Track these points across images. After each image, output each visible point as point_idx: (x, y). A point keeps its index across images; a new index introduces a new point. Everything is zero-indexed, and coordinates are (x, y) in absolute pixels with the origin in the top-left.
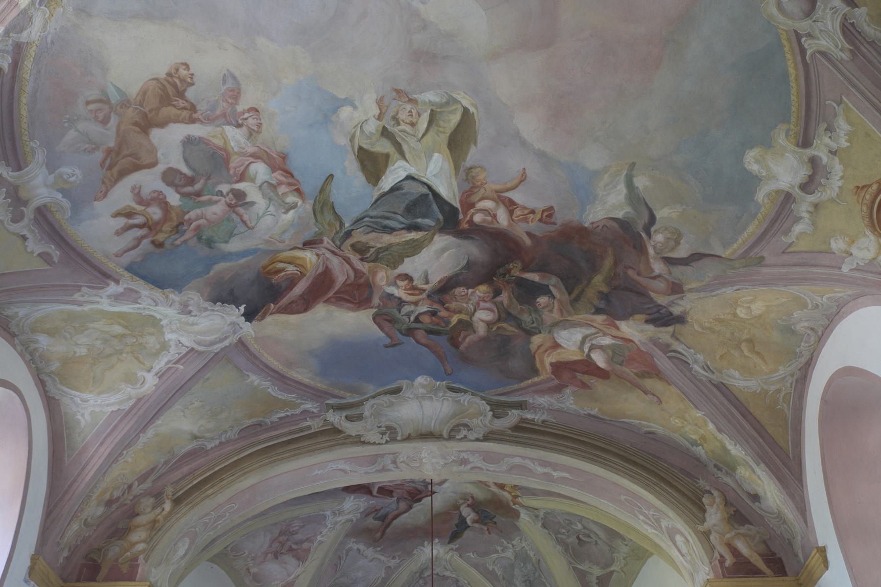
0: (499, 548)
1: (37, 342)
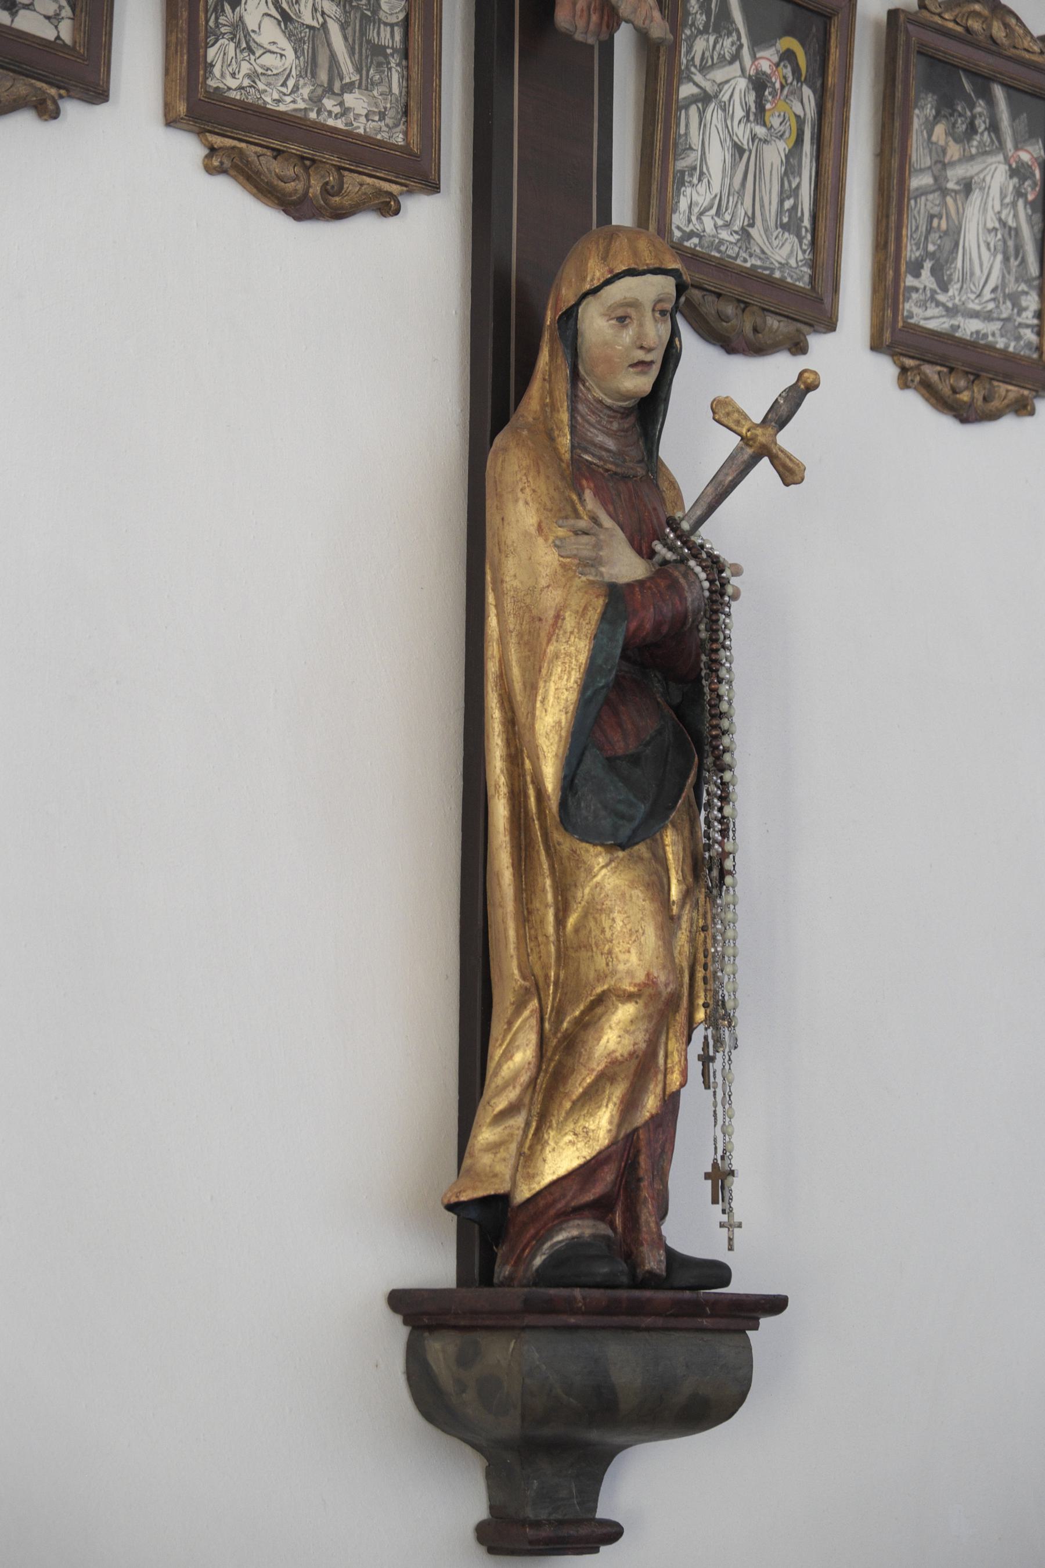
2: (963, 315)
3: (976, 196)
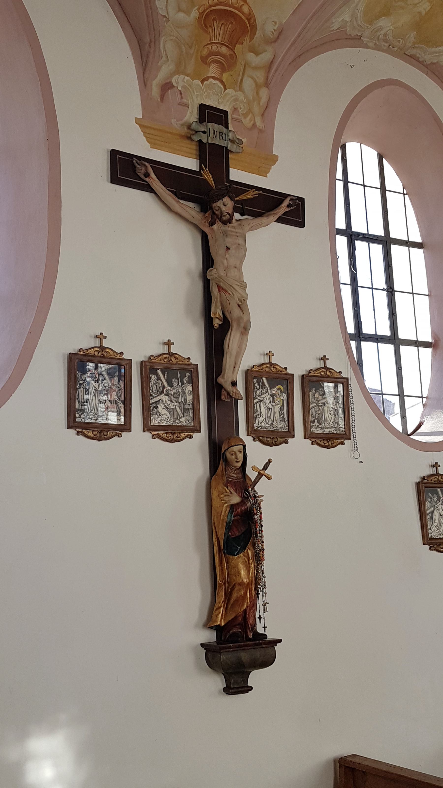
1: (381, 28)
2: (325, 428)
3: (326, 405)
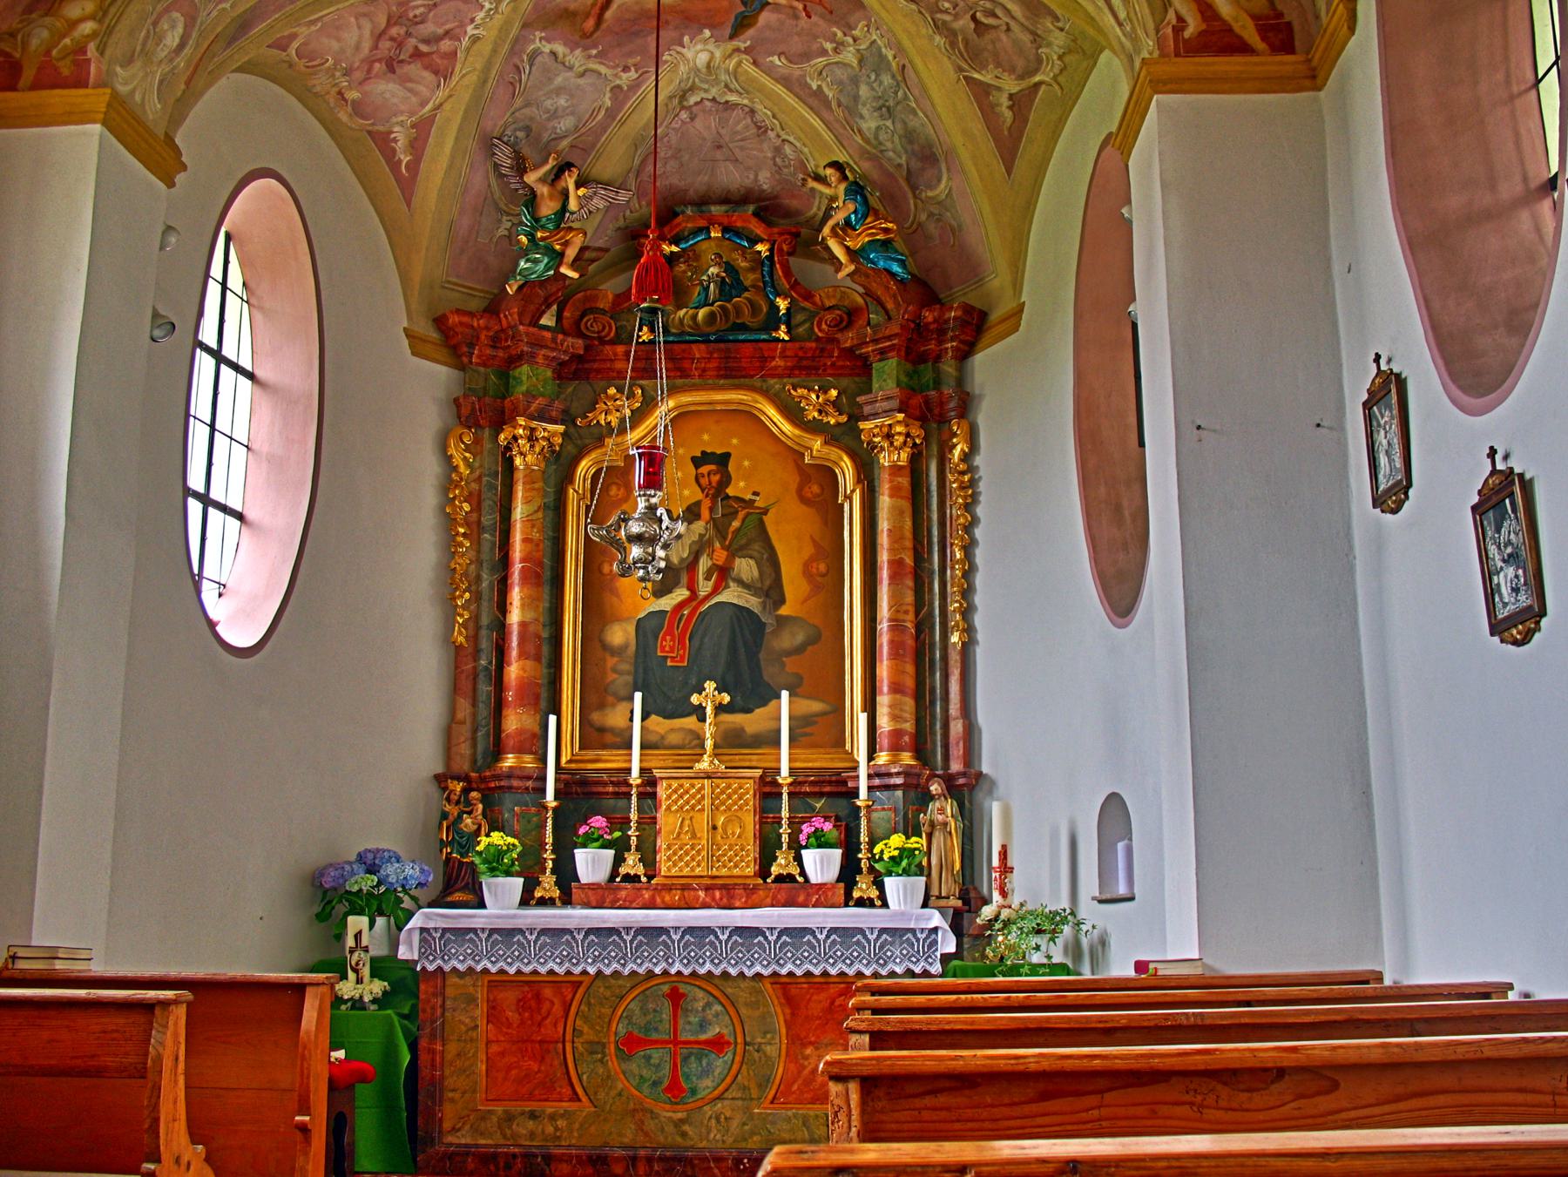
0: (829, 46)
